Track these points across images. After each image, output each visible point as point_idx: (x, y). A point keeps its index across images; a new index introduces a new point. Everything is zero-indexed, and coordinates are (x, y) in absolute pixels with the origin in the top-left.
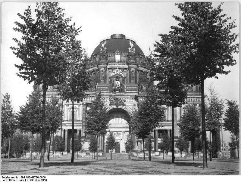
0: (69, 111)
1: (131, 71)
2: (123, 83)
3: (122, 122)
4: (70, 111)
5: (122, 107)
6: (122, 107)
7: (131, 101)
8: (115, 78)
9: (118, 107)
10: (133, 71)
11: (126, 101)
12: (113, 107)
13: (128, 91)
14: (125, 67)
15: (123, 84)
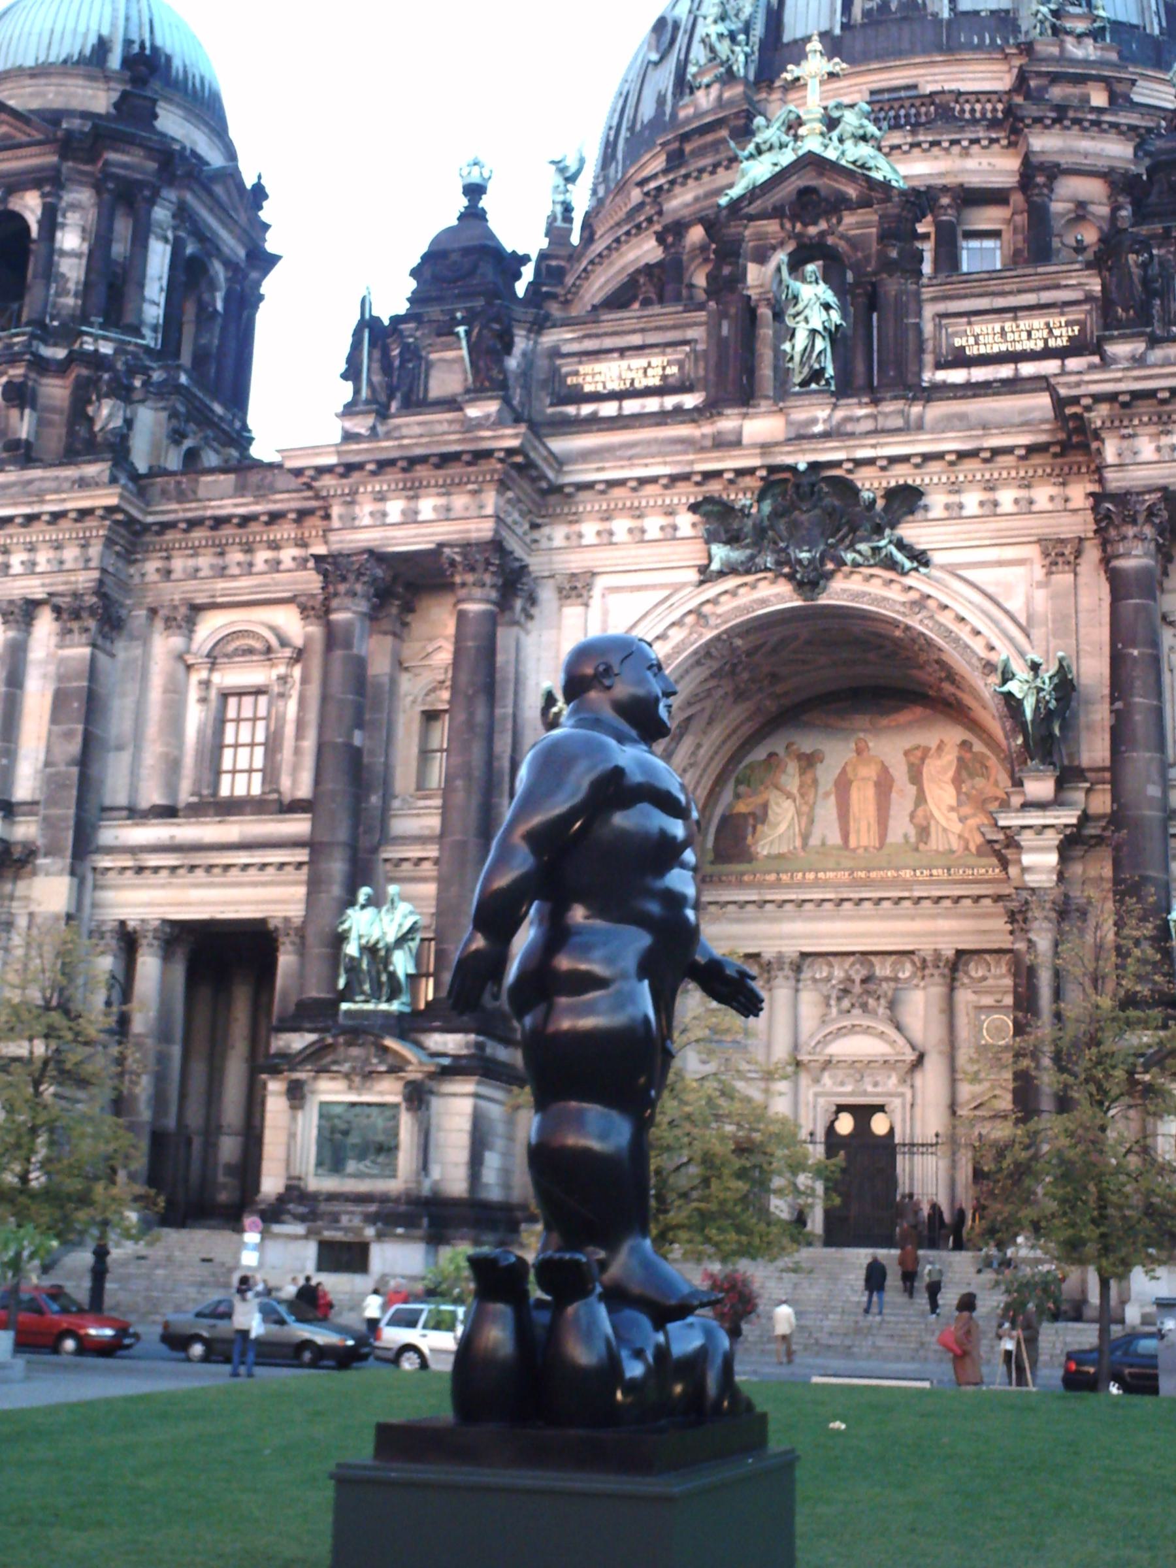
0: (193, 694)
1: (1057, 207)
2: (888, 266)
3: (924, 832)
4: (206, 684)
5: (875, 588)
6: (875, 588)
7: (1007, 497)
8: (776, 212)
9: (823, 600)
10: (1081, 205)
11: (937, 501)
12: (746, 597)
13: (957, 376)
14: (975, 181)
15: (892, 286)
